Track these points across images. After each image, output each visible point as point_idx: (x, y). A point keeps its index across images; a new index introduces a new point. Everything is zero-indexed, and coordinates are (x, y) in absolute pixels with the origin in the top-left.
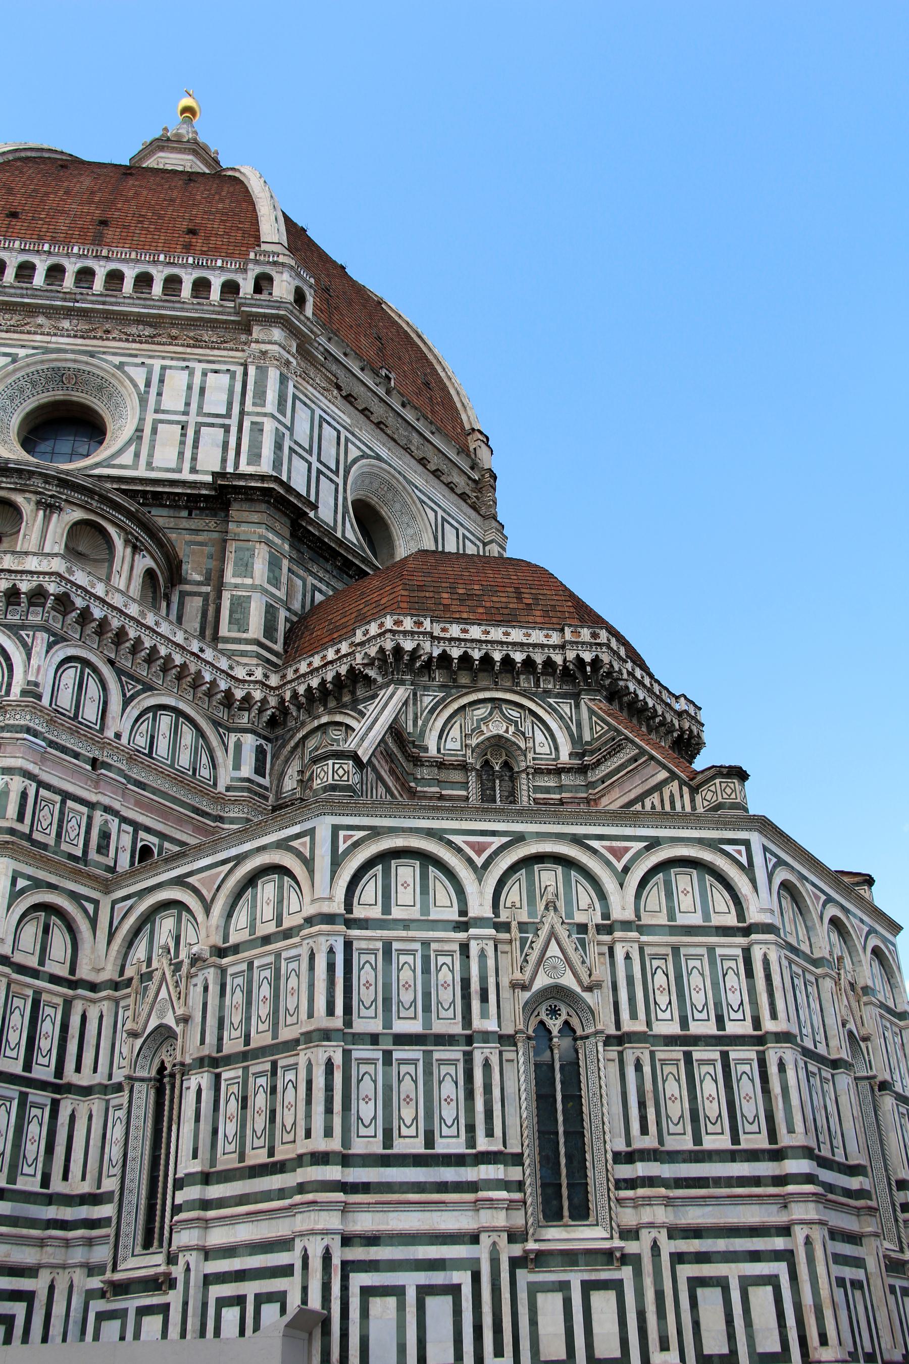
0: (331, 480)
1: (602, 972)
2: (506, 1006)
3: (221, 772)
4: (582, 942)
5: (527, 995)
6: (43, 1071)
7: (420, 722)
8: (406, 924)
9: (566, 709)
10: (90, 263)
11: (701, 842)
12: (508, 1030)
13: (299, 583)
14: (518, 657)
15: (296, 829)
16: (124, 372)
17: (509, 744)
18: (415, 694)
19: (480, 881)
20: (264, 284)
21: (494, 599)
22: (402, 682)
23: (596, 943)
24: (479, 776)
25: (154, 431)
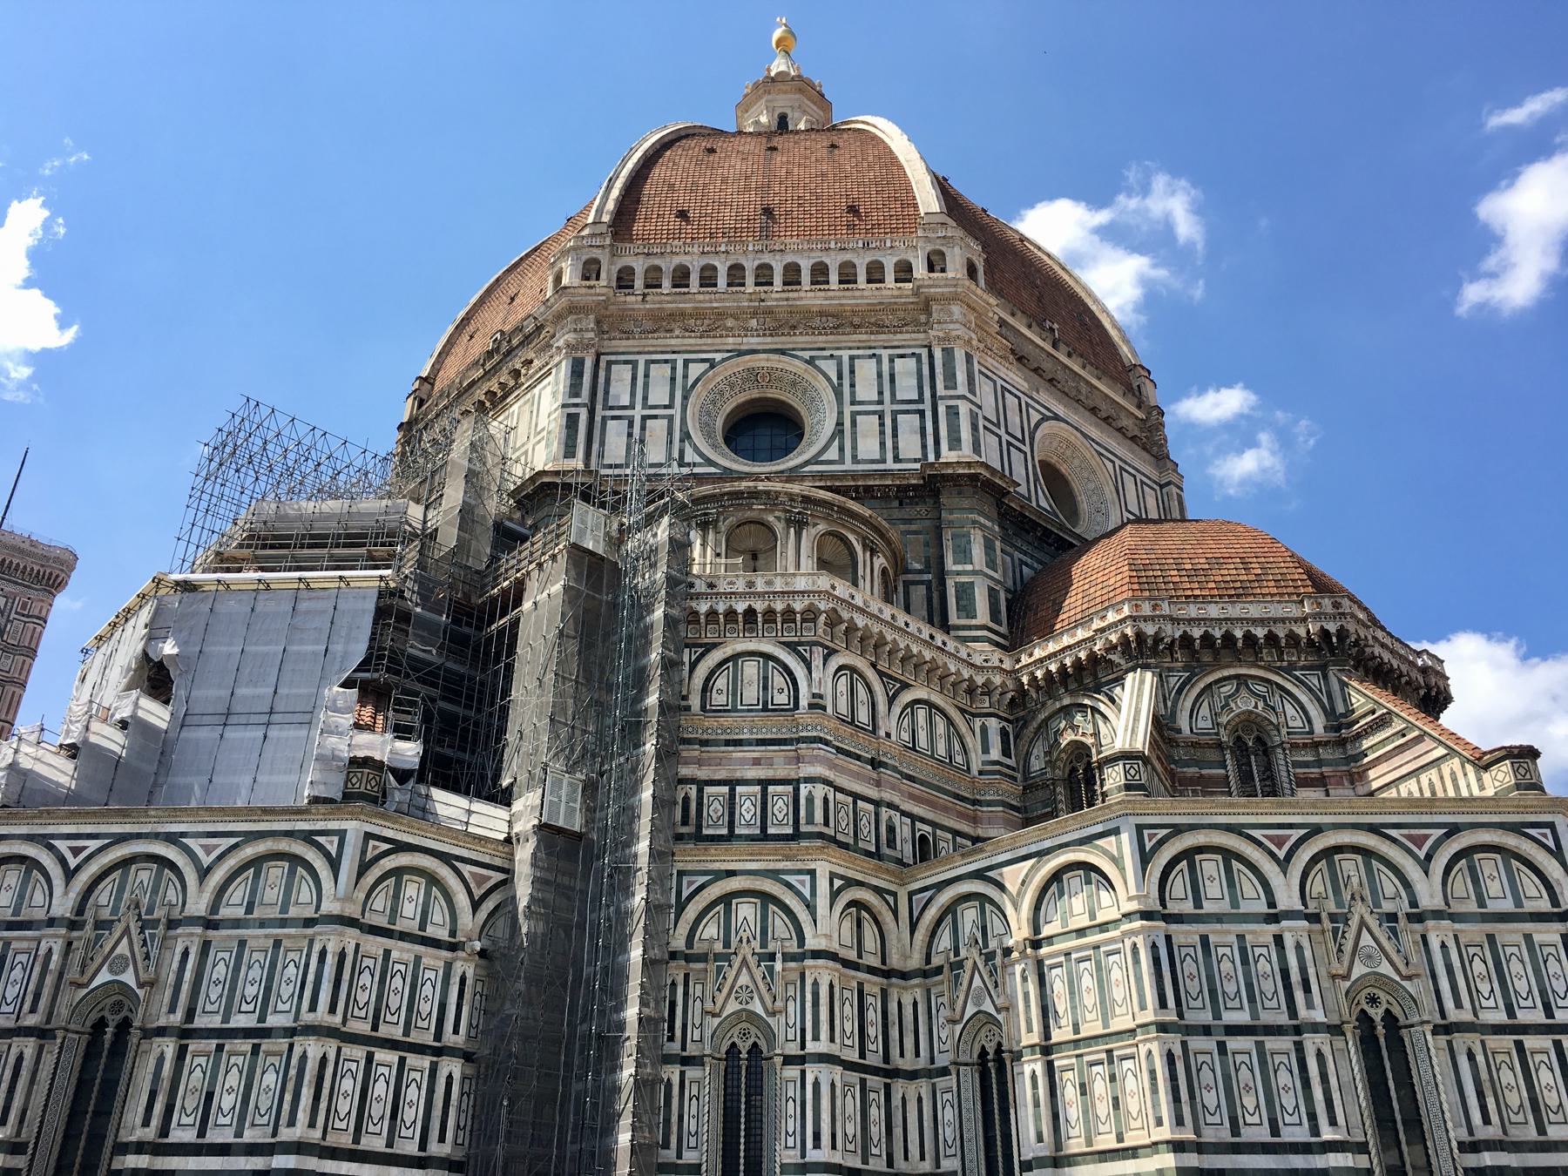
0: (1020, 450)
2: (1329, 996)
3: (973, 756)
4: (1394, 931)
5: (1348, 984)
6: (874, 1060)
7: (1169, 704)
8: (1218, 918)
10: (766, 258)
13: (1008, 559)
16: (816, 367)
17: (1259, 719)
18: (1161, 676)
22: (1146, 667)
23: (1409, 934)
24: (1232, 753)
25: (854, 423)
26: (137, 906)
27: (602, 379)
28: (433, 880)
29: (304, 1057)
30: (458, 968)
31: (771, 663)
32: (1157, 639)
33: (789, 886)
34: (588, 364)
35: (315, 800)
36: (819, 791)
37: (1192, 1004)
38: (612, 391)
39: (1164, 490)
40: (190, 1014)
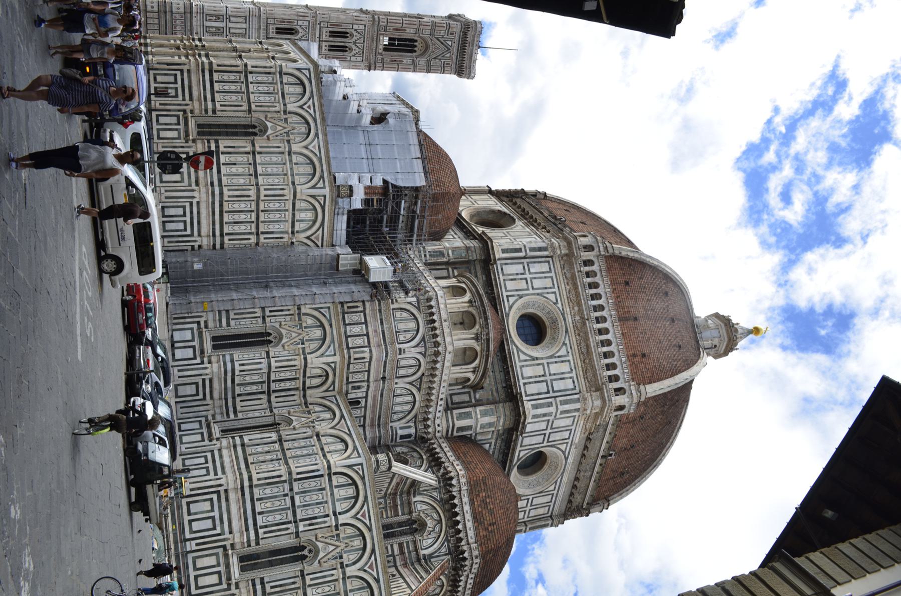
0: (544, 440)
1: (326, 566)
3: (398, 423)
5: (314, 540)
6: (273, 386)
8: (332, 494)
9: (443, 550)
10: (609, 320)
12: (301, 535)
13: (490, 437)
14: (460, 527)
15: (360, 451)
16: (562, 346)
18: (436, 488)
22: (439, 483)
24: (409, 520)
27: (540, 260)
28: (315, 222)
29: (250, 190)
30: (285, 236)
32: (451, 485)
33: (329, 347)
34: (545, 253)
35: (335, 178)
36: (367, 355)
37: (300, 485)
38: (536, 265)
40: (260, 153)
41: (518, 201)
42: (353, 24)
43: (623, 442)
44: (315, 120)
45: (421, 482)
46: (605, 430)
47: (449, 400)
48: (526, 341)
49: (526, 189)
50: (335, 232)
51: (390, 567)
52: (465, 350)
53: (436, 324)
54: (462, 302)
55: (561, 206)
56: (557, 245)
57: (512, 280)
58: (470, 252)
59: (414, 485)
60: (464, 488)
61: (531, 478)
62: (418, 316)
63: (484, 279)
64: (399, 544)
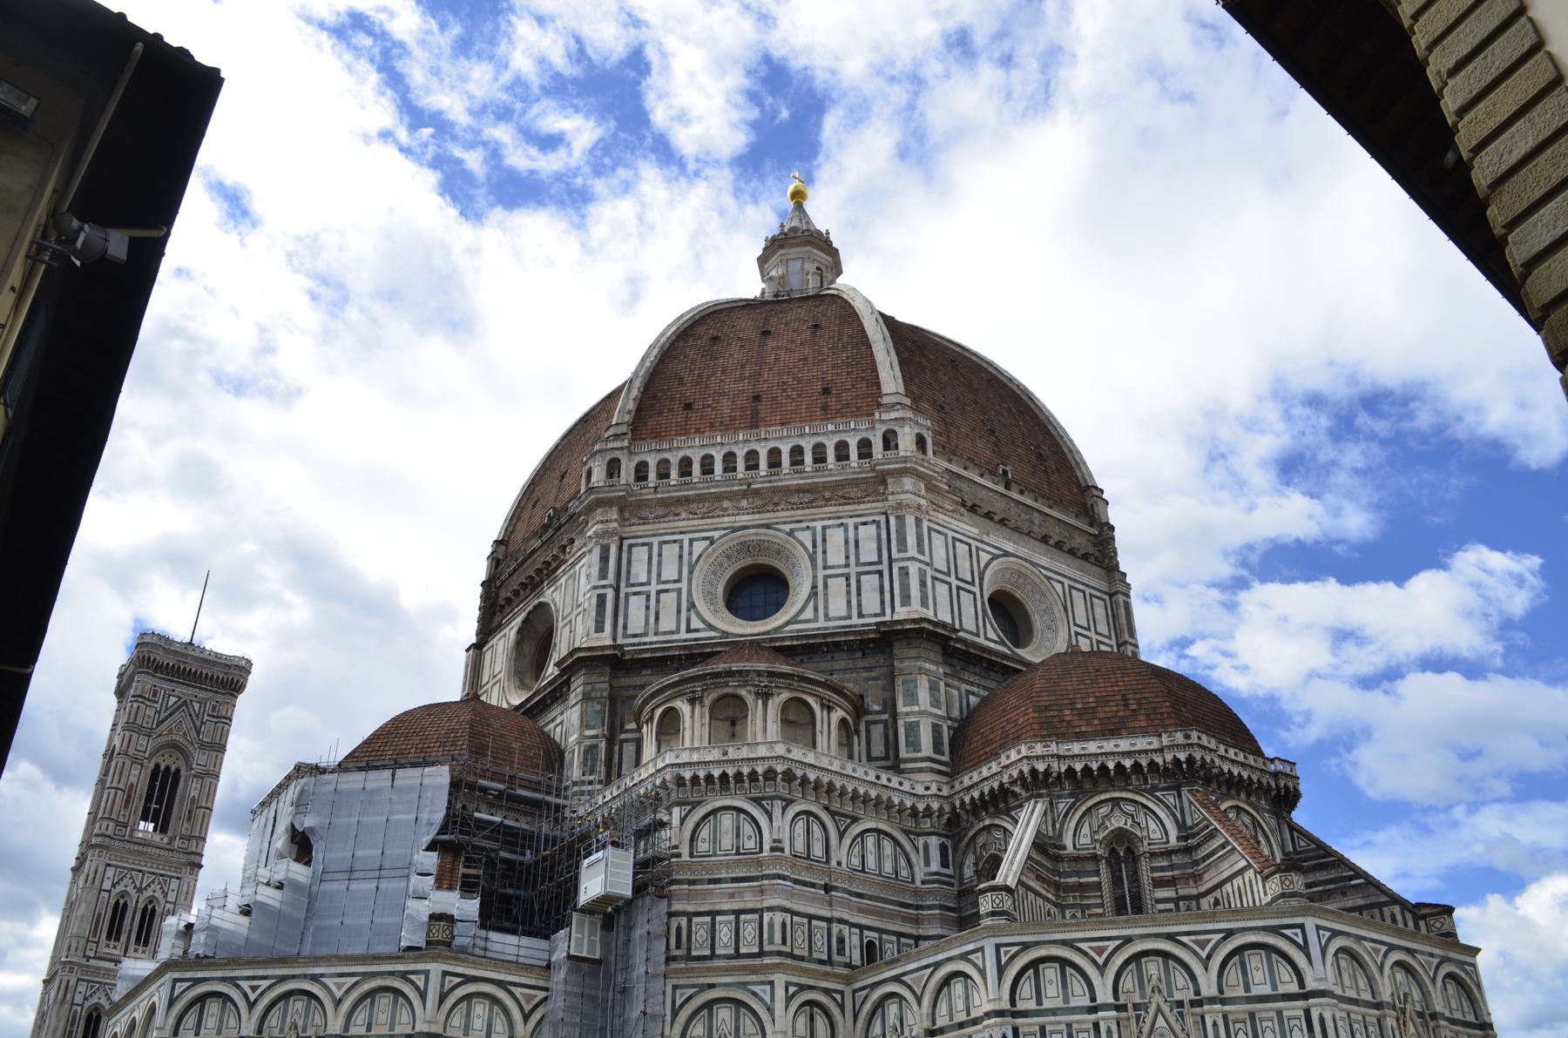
0: (969, 592)
3: (917, 869)
7: (1058, 826)
8: (1054, 1012)
9: (1171, 800)
10: (754, 446)
11: (1265, 929)
13: (955, 692)
14: (1128, 763)
15: (971, 947)
16: (795, 538)
18: (1051, 803)
19: (1102, 976)
20: (890, 436)
21: (1107, 709)
22: (1040, 796)
24: (1108, 863)
25: (826, 586)
26: (296, 1028)
27: (624, 561)
28: (494, 1000)
31: (742, 816)
32: (1047, 772)
33: (754, 994)
34: (613, 549)
35: (409, 949)
36: (778, 917)
38: (633, 570)
39: (1114, 599)
41: (504, 594)
42: (101, 890)
43: (983, 447)
44: (282, 979)
45: (1038, 831)
46: (959, 476)
47: (879, 763)
48: (778, 605)
49: (483, 577)
50: (521, 960)
51: (1199, 908)
52: (786, 722)
53: (731, 771)
54: (692, 717)
55: (525, 516)
56: (600, 526)
57: (657, 619)
58: (593, 694)
59: (1043, 845)
60: (1053, 748)
61: (1038, 624)
62: (709, 807)
63: (649, 672)
64: (1155, 887)
